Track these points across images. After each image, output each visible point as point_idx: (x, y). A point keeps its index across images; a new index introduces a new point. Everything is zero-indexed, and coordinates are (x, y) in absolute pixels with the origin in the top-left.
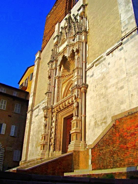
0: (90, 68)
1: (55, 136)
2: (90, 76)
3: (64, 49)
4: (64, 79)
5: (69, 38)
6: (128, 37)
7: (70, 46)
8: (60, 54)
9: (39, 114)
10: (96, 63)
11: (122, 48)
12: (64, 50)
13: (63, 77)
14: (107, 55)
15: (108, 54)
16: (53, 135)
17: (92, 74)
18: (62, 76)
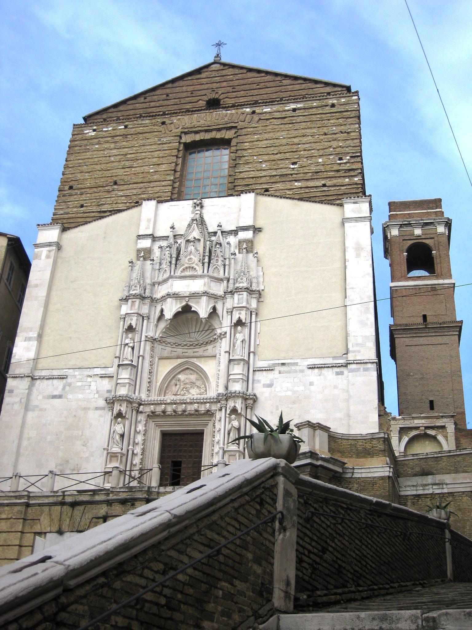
0: (265, 370)
1: (141, 463)
2: (262, 383)
3: (193, 294)
4: (163, 347)
5: (211, 277)
6: (359, 366)
7: (211, 296)
8: (175, 296)
9: (70, 396)
10: (282, 368)
11: (342, 373)
12: (192, 295)
13: (161, 343)
14: (310, 368)
15: (312, 367)
16: (137, 460)
17: (268, 382)
18: (159, 341)
